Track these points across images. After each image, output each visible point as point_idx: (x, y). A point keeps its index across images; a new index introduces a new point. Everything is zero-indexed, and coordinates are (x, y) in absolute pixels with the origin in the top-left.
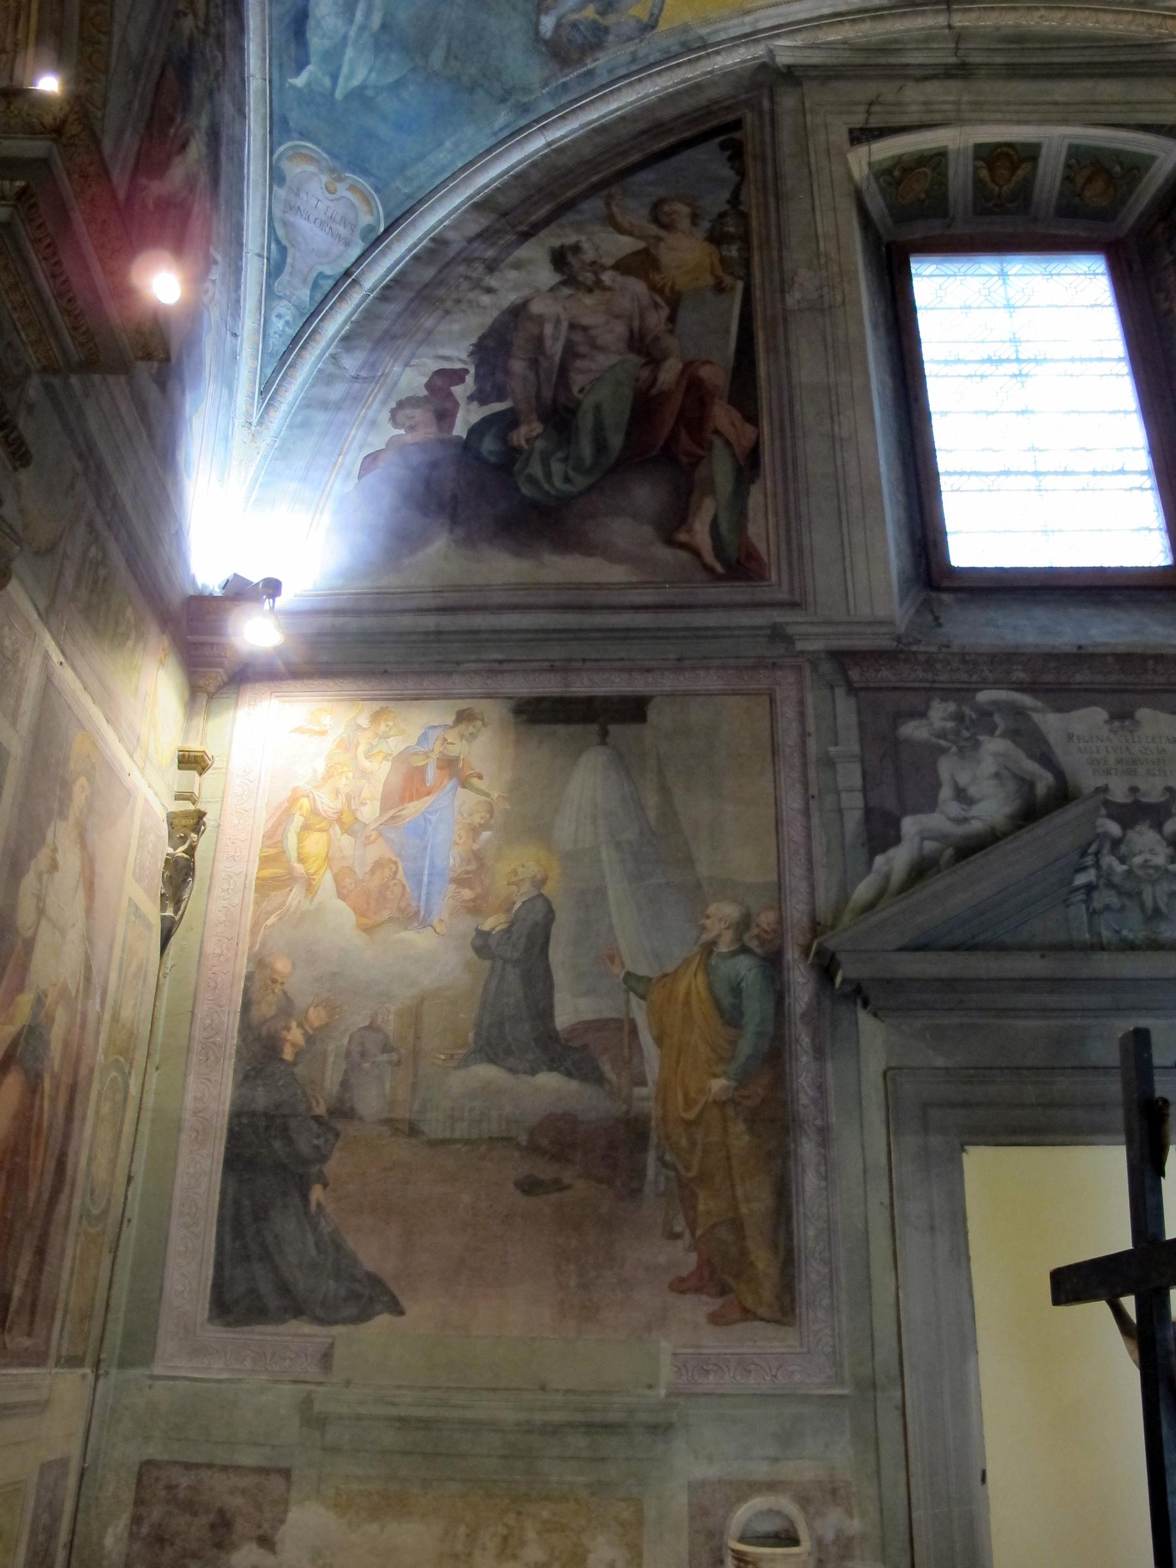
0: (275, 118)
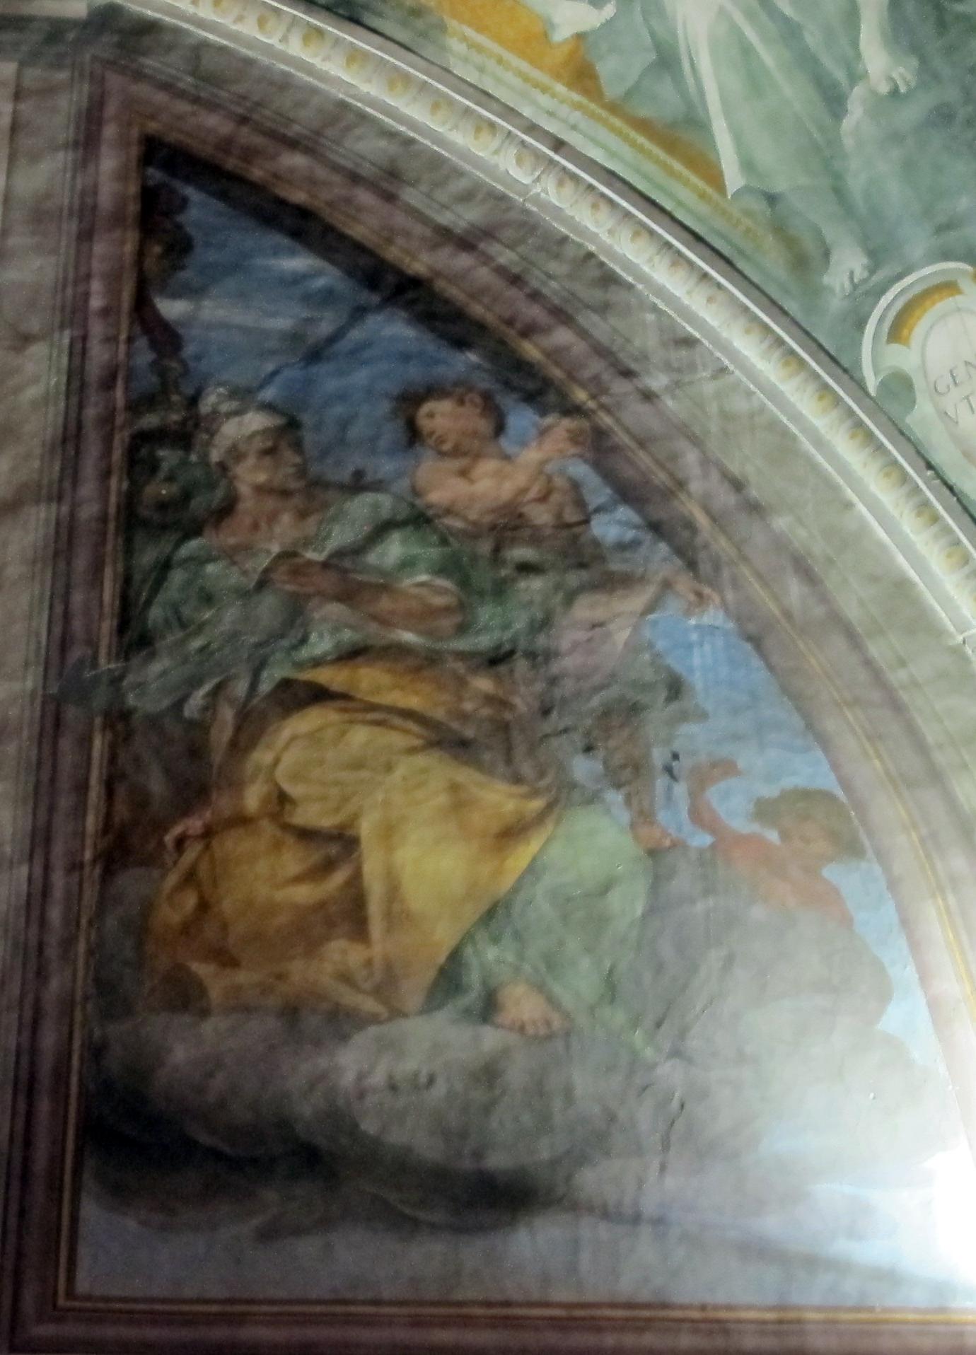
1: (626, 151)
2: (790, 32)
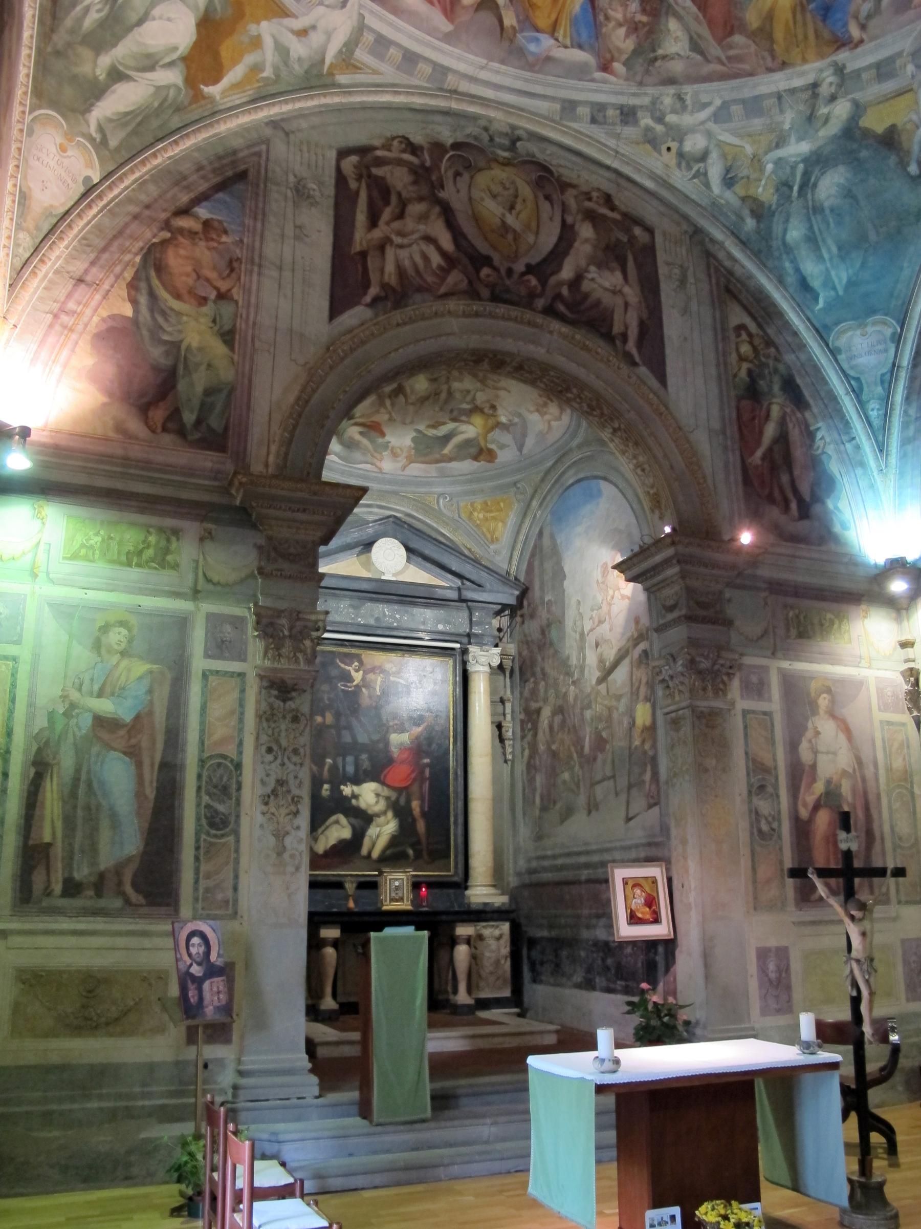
0: (821, 329)
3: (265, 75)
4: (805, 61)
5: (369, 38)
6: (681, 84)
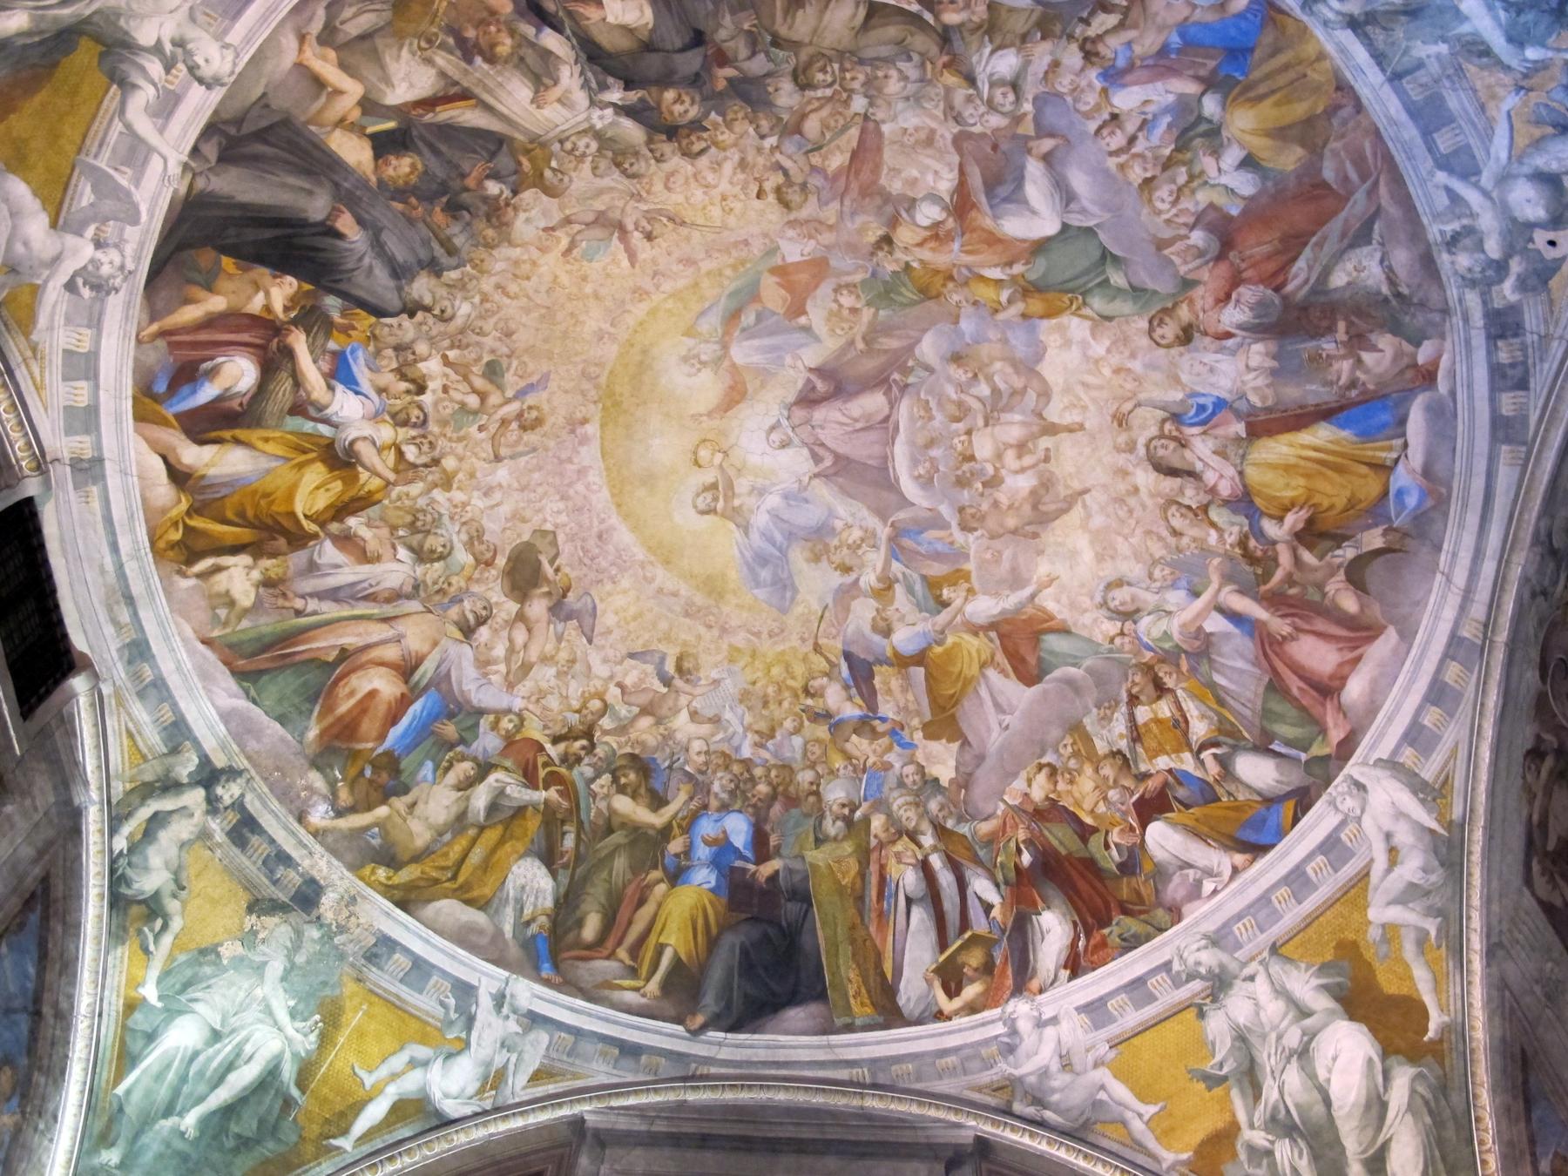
1: (110, 1040)
2: (183, 1079)
3: (1433, 933)
4: (1322, 56)
5: (1408, 756)
6: (1429, 245)
